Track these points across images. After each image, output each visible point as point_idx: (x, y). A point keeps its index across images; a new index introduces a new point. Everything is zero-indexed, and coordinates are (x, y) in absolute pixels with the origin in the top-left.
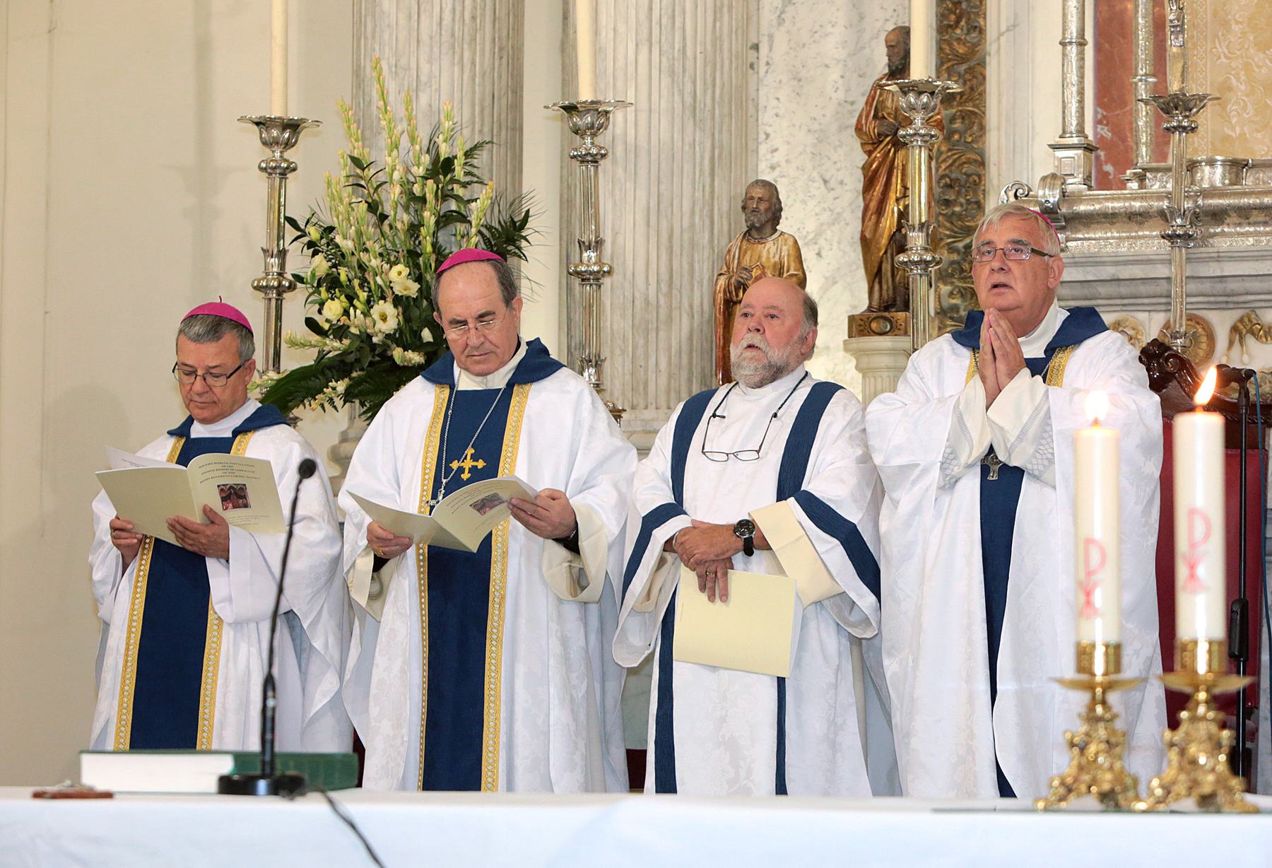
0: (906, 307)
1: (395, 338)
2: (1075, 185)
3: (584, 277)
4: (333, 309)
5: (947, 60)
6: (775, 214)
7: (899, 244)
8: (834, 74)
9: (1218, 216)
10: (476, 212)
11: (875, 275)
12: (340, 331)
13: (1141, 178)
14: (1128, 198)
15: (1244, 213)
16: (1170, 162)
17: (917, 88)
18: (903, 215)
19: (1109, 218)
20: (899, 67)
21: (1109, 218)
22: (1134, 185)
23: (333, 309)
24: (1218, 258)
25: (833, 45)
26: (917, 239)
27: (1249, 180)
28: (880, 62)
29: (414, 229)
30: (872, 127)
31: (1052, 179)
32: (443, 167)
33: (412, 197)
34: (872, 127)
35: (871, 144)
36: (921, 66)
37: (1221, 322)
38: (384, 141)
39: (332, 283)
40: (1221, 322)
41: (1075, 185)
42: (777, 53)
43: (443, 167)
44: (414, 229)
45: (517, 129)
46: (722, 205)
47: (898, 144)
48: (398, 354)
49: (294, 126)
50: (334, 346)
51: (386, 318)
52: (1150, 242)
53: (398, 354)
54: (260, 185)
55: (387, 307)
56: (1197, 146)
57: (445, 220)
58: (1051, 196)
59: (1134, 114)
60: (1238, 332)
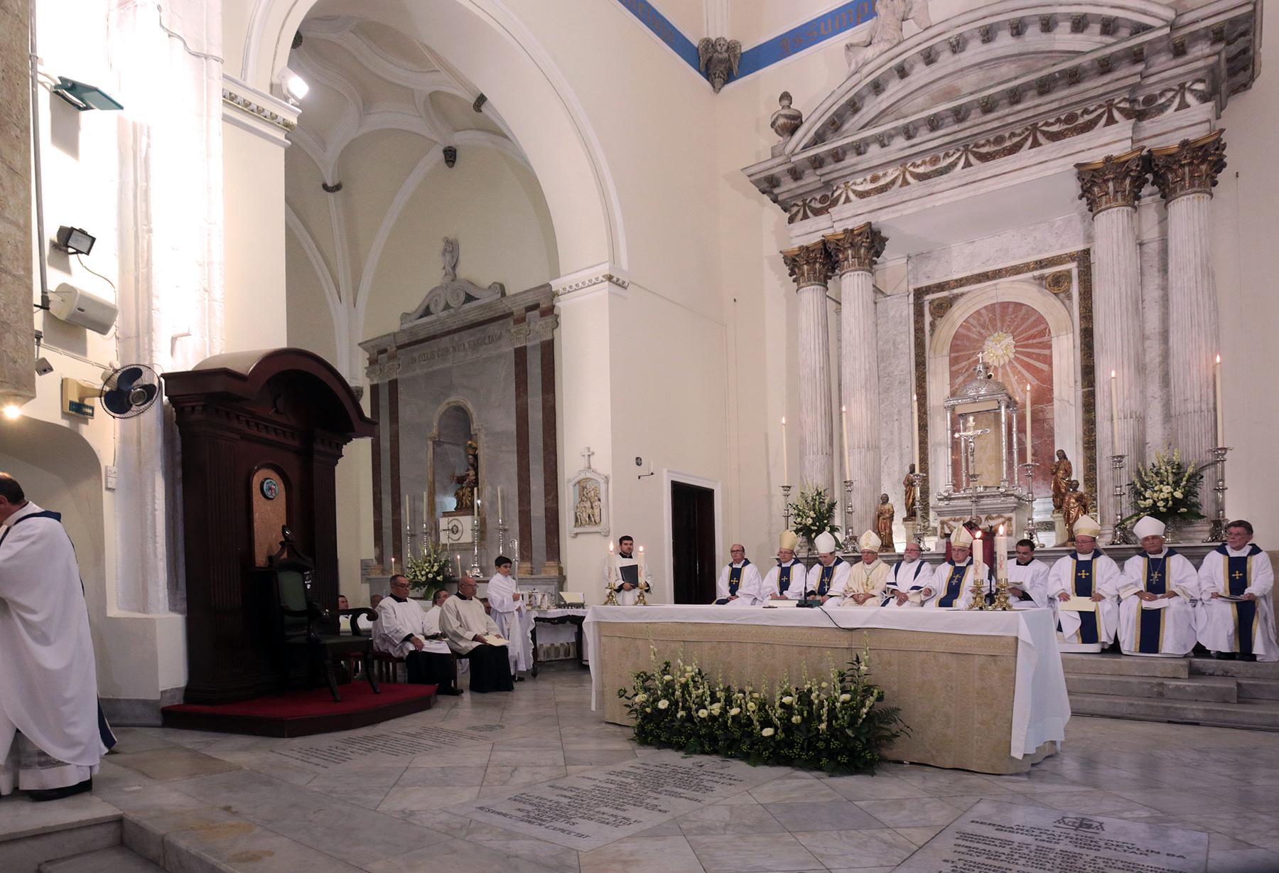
0: (915, 516)
1: (812, 525)
2: (951, 492)
3: (849, 513)
4: (799, 520)
5: (921, 470)
6: (888, 500)
7: (913, 504)
8: (897, 473)
9: (982, 497)
10: (826, 501)
11: (908, 510)
12: (800, 524)
13: (964, 490)
14: (962, 494)
15: (988, 496)
16: (971, 486)
17: (918, 475)
18: (914, 499)
19: (959, 498)
20: (912, 470)
21: (959, 498)
22: (962, 492)
23: (799, 520)
24: (983, 505)
25: (896, 468)
26: (917, 503)
27: (988, 490)
28: (907, 470)
29: (814, 505)
30: (907, 483)
31: (946, 491)
32: (819, 494)
33: (813, 498)
34: (907, 483)
35: (906, 486)
36: (917, 471)
37: (983, 517)
38: (807, 489)
39: (799, 515)
40: (983, 517)
41: (951, 492)
42: (885, 470)
43: (819, 494)
44: (814, 505)
45: (833, 486)
46: (876, 498)
47: (913, 486)
48: (812, 527)
49: (789, 487)
50: (799, 526)
51: (810, 521)
52: (968, 502)
53: (812, 527)
54: (783, 498)
55: (810, 519)
56: (977, 484)
57: (820, 503)
58: (946, 494)
59: (962, 478)
60: (986, 519)
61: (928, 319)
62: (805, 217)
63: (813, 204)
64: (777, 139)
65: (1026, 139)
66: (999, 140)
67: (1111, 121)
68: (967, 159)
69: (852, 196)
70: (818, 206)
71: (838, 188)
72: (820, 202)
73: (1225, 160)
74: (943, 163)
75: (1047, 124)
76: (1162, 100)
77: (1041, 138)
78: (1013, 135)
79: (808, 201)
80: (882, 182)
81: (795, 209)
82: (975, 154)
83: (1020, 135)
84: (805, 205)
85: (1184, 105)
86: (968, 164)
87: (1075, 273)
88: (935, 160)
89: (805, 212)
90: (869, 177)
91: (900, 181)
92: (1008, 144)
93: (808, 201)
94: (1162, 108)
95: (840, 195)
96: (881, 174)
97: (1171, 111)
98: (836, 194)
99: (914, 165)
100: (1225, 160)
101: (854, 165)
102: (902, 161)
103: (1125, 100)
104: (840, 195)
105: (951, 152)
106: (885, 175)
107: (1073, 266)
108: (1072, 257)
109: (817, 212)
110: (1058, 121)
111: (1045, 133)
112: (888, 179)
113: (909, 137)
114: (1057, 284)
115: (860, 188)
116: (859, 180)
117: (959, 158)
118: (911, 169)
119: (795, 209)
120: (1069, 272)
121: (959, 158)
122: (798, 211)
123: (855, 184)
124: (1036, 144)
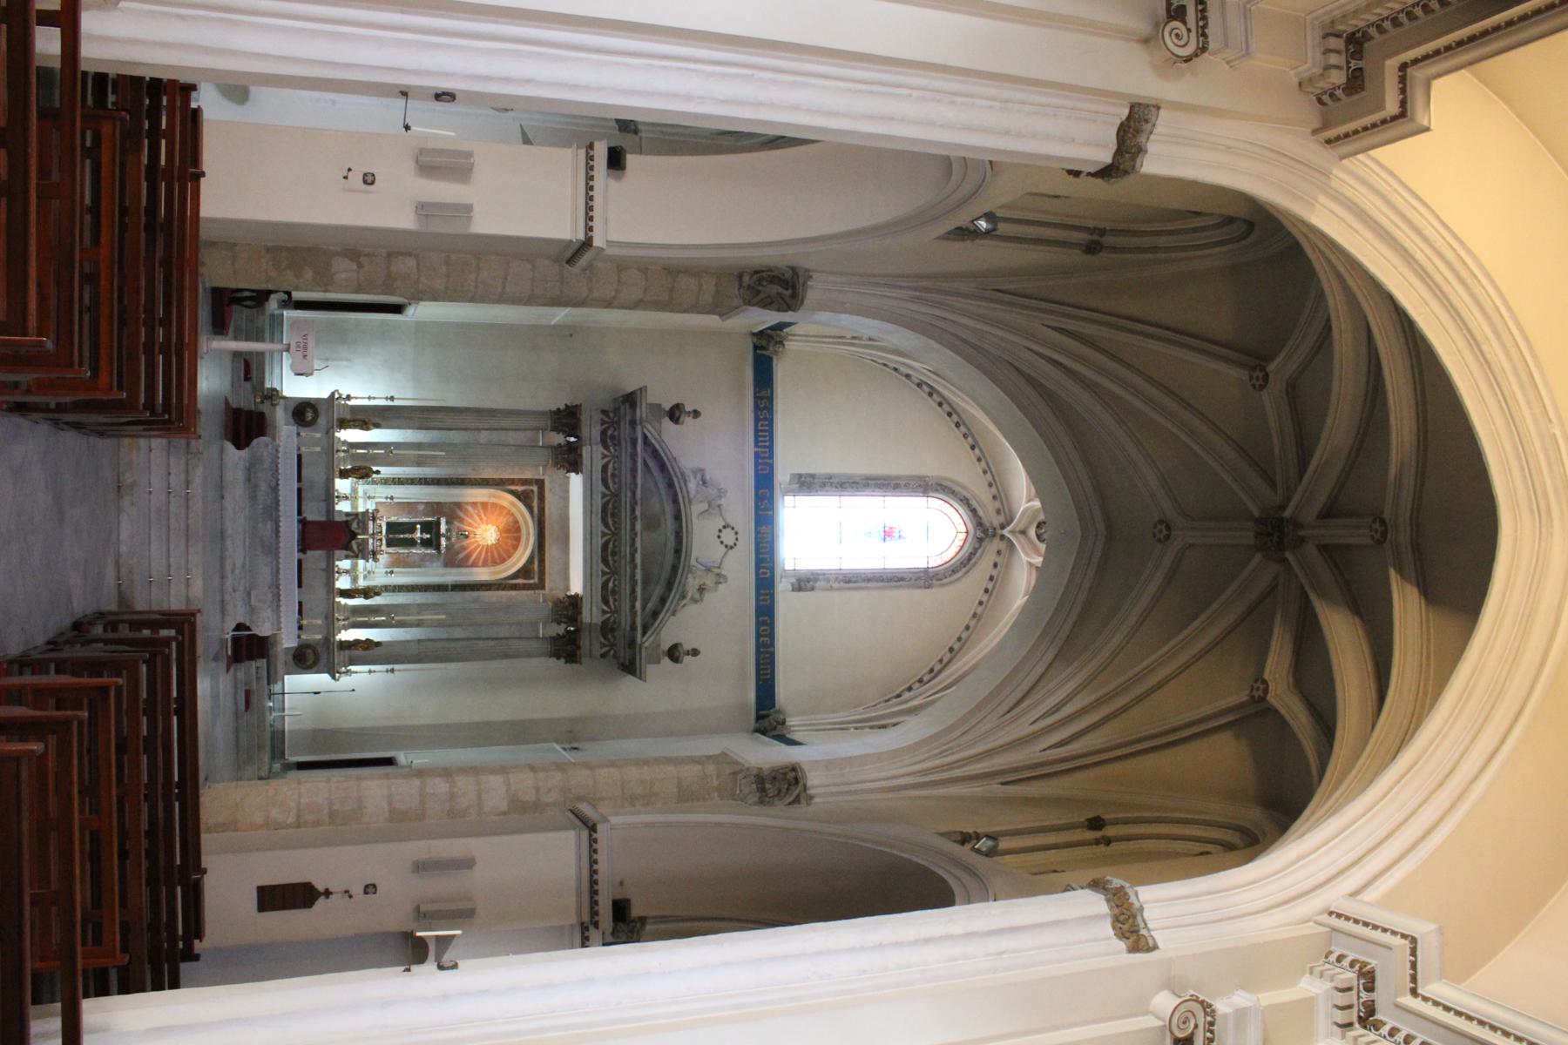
61: (520, 488)
62: (603, 423)
63: (612, 429)
66: (614, 553)
67: (604, 612)
68: (607, 534)
69: (606, 460)
70: (610, 432)
73: (563, 660)
75: (615, 580)
76: (610, 636)
77: (606, 577)
78: (615, 561)
80: (610, 481)
81: (611, 415)
82: (610, 539)
84: (613, 422)
85: (603, 646)
88: (613, 515)
90: (616, 472)
92: (610, 558)
94: (605, 637)
95: (610, 451)
96: (617, 480)
97: (603, 640)
98: (612, 449)
100: (563, 660)
104: (610, 451)
109: (604, 433)
110: (615, 586)
111: (609, 580)
112: (611, 485)
115: (611, 466)
117: (610, 530)
119: (611, 415)
121: (610, 530)
122: (609, 417)
124: (604, 573)
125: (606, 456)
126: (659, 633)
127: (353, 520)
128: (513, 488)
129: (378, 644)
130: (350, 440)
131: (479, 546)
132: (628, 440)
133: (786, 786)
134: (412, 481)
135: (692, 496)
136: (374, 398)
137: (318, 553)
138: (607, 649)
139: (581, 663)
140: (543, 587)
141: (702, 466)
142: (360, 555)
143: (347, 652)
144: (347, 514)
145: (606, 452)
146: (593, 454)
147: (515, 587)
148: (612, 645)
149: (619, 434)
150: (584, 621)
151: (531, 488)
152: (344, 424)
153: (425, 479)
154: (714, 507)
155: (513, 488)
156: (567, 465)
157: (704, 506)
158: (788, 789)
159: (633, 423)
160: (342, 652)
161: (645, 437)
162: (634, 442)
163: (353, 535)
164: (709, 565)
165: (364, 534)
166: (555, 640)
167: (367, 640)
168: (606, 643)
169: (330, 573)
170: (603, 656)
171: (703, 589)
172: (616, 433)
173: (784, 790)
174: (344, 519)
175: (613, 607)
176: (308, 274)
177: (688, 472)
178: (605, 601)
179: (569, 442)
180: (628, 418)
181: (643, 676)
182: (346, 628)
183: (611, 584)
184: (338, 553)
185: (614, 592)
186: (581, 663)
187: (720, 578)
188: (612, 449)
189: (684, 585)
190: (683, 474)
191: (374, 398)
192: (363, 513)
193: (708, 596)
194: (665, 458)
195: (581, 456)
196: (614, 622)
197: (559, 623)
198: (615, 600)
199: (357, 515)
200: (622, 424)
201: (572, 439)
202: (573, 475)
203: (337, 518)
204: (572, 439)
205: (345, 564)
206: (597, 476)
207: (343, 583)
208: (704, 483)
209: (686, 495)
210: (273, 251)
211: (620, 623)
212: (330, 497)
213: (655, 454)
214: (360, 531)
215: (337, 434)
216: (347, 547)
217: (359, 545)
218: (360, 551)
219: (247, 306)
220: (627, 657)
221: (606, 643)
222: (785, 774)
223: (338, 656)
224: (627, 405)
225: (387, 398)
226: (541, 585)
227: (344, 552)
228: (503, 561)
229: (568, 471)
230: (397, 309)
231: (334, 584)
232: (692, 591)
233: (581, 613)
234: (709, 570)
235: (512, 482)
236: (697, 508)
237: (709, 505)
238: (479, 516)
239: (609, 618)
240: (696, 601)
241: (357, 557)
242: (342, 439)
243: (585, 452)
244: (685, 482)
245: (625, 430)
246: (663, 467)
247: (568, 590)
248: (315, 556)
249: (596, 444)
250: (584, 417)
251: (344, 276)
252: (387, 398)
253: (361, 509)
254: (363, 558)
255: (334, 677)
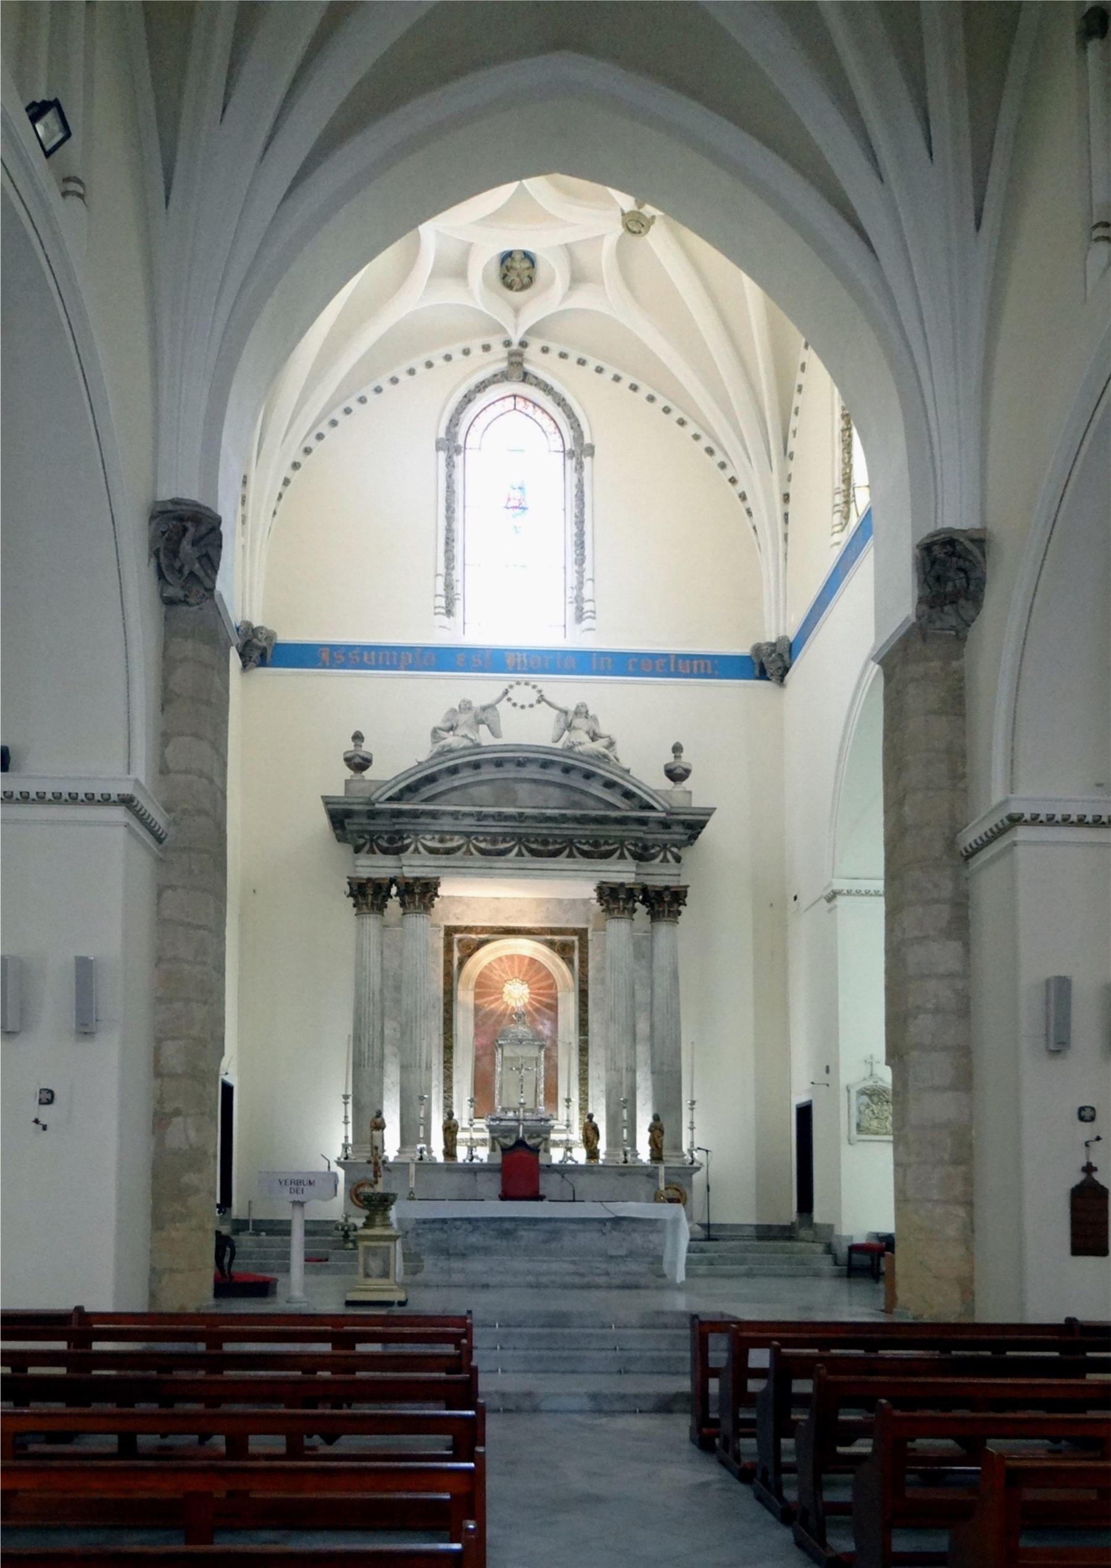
63: (380, 842)
64: (348, 773)
65: (564, 848)
66: (545, 843)
67: (622, 856)
68: (520, 849)
70: (385, 844)
71: (408, 837)
72: (387, 842)
74: (502, 846)
75: (580, 843)
79: (375, 838)
80: (449, 845)
83: (561, 843)
86: (520, 854)
87: (577, 944)
88: (494, 842)
89: (371, 848)
91: (464, 849)
92: (551, 847)
93: (375, 838)
98: (407, 841)
99: (476, 839)
101: (427, 824)
102: (468, 835)
103: (632, 844)
105: (508, 839)
106: (452, 840)
107: (575, 938)
108: (575, 932)
109: (385, 851)
110: (587, 843)
111: (578, 849)
112: (454, 844)
113: (479, 820)
114: (564, 951)
115: (429, 844)
116: (428, 837)
117: (514, 846)
118: (474, 841)
119: (361, 841)
120: (573, 942)
121: (514, 846)
123: (423, 838)
124: (571, 855)
125: (416, 850)
126: (655, 791)
127: (499, 1143)
128: (456, 962)
129: (656, 1118)
130: (398, 1145)
131: (534, 999)
132: (395, 820)
133: (955, 559)
134: (448, 1078)
135: (470, 744)
136: (346, 1117)
137: (542, 1184)
138: (669, 856)
139: (687, 886)
140: (585, 930)
141: (430, 730)
142: (544, 1136)
143: (665, 1153)
144: (493, 1149)
145: (412, 848)
146: (414, 866)
147: (584, 962)
148: (664, 848)
149: (386, 832)
150: (632, 881)
151: (455, 940)
152: (377, 1149)
153: (445, 1062)
154: (485, 716)
155: (456, 962)
156: (428, 895)
157: (483, 728)
158: (960, 557)
159: (373, 815)
160: (664, 1158)
161: (390, 799)
162: (399, 814)
163: (520, 1143)
164: (562, 725)
165: (518, 1133)
166: (655, 916)
167: (650, 1130)
168: (661, 856)
169: (564, 1170)
170: (678, 859)
171: (595, 734)
172: (386, 837)
173: (961, 563)
174: (499, 1152)
175: (616, 846)
176: (191, 1178)
177: (437, 748)
178: (606, 855)
179: (397, 895)
180: (365, 821)
181: (710, 811)
182: (636, 1154)
183: (586, 848)
184: (542, 1160)
185: (596, 844)
186: (687, 886)
187: (581, 711)
188: (407, 841)
189: (590, 756)
190: (440, 754)
191: (346, 1117)
192: (491, 1132)
193: (604, 729)
194: (419, 776)
195: (417, 879)
196: (636, 845)
197: (634, 910)
198: (606, 843)
199: (493, 1139)
200: (372, 828)
201: (394, 890)
202: (441, 891)
203: (498, 1159)
204: (394, 890)
205: (556, 1155)
206: (442, 860)
207: (580, 1155)
208: (452, 728)
209: (467, 752)
210: (158, 1221)
211: (638, 838)
212: (473, 1169)
213: (412, 789)
214: (514, 1136)
215: (391, 1159)
216: (535, 1150)
217: (530, 1137)
218: (539, 1136)
219: (232, 1258)
220: (682, 831)
221: (661, 856)
222: (933, 562)
223: (670, 1160)
224: (346, 821)
225: (346, 1103)
226: (582, 933)
227: (541, 1154)
228: (549, 975)
229: (436, 895)
230: (227, 1090)
231: (582, 1166)
232: (599, 746)
233: (622, 885)
234: (569, 727)
235: (448, 962)
236: (485, 737)
237: (483, 722)
238: (492, 1002)
239: (629, 850)
240: (611, 744)
241: (546, 1140)
242: (397, 1154)
243: (409, 873)
244: (451, 751)
245: (381, 824)
246: (431, 779)
247: (586, 902)
248: (548, 1184)
249: (400, 860)
250: (364, 873)
251: (192, 1133)
252: (346, 1103)
253: (486, 1135)
254: (548, 1132)
255: (698, 1169)
